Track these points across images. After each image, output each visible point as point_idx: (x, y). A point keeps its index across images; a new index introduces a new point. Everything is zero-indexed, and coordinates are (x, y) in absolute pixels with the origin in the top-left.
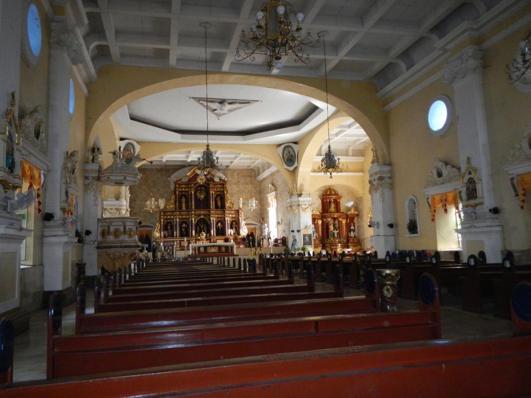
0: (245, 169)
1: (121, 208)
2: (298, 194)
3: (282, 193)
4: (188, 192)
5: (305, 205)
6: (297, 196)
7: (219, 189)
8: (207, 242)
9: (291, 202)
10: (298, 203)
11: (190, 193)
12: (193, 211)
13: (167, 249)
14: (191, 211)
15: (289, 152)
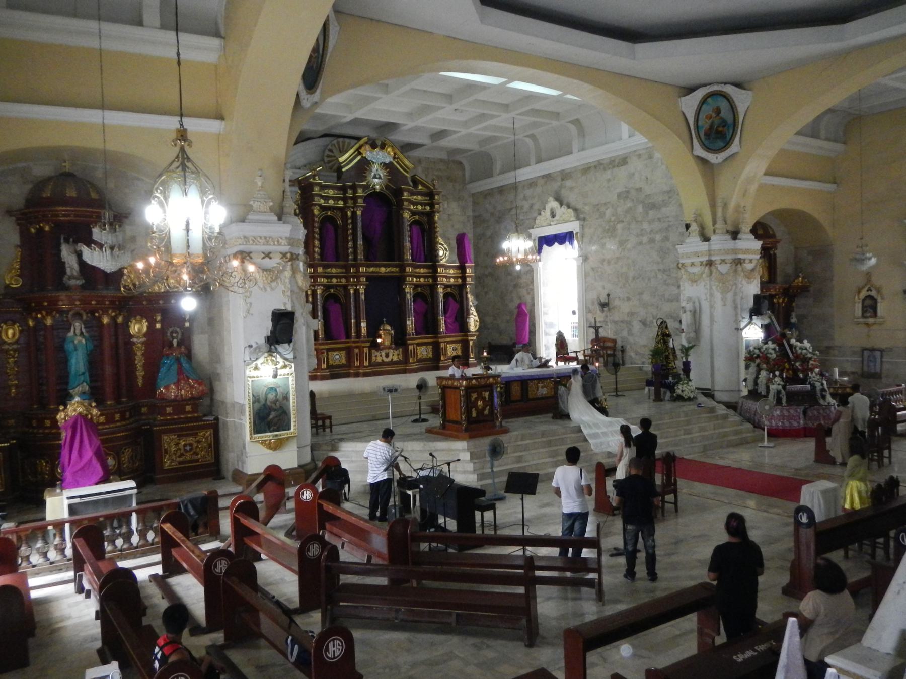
0: (441, 161)
1: (297, 253)
2: (728, 232)
3: (619, 226)
4: (342, 210)
5: (751, 261)
6: (728, 237)
7: (420, 207)
8: (396, 352)
9: (710, 253)
10: (734, 257)
11: (349, 214)
12: (363, 265)
13: (477, 400)
14: (357, 266)
15: (718, 111)
